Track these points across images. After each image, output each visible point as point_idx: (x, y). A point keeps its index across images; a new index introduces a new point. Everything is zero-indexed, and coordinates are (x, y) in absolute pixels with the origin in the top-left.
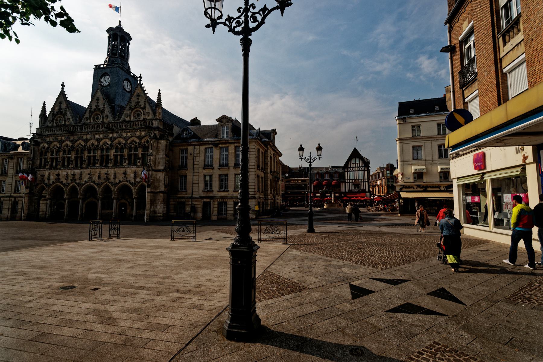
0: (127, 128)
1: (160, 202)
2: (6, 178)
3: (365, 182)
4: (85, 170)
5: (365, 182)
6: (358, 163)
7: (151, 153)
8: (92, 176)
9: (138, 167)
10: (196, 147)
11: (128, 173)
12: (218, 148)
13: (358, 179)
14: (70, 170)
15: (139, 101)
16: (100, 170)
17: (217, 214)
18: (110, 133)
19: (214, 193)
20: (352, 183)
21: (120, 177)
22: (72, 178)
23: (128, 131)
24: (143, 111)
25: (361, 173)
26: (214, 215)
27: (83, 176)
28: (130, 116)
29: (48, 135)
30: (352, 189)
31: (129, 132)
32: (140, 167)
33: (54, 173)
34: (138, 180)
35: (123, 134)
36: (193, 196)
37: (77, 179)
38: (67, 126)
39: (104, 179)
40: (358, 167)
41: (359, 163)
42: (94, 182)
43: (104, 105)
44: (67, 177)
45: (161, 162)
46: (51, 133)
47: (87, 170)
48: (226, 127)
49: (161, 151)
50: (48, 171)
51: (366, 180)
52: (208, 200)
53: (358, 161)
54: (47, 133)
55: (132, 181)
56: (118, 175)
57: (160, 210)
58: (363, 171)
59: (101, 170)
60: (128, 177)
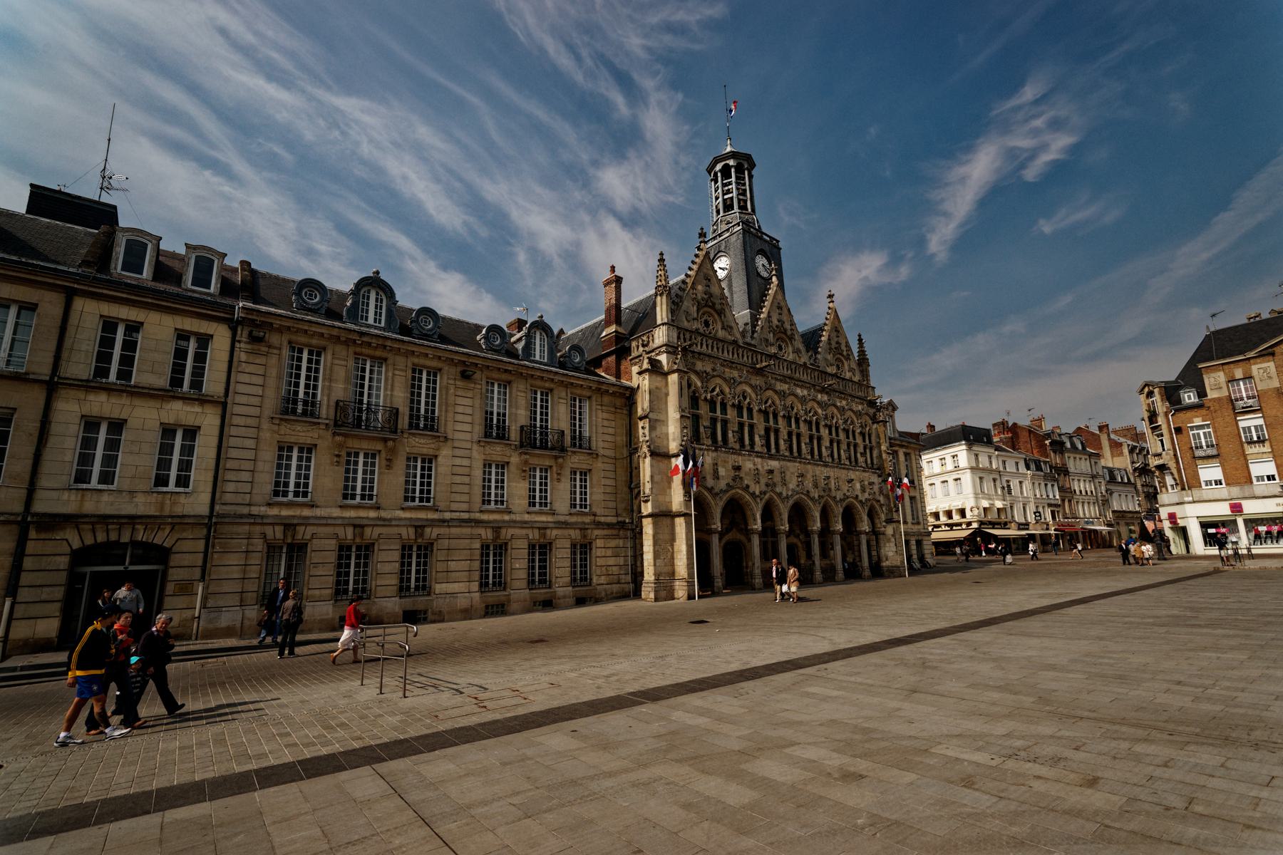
2: (438, 449)
29: (700, 354)
44: (757, 473)
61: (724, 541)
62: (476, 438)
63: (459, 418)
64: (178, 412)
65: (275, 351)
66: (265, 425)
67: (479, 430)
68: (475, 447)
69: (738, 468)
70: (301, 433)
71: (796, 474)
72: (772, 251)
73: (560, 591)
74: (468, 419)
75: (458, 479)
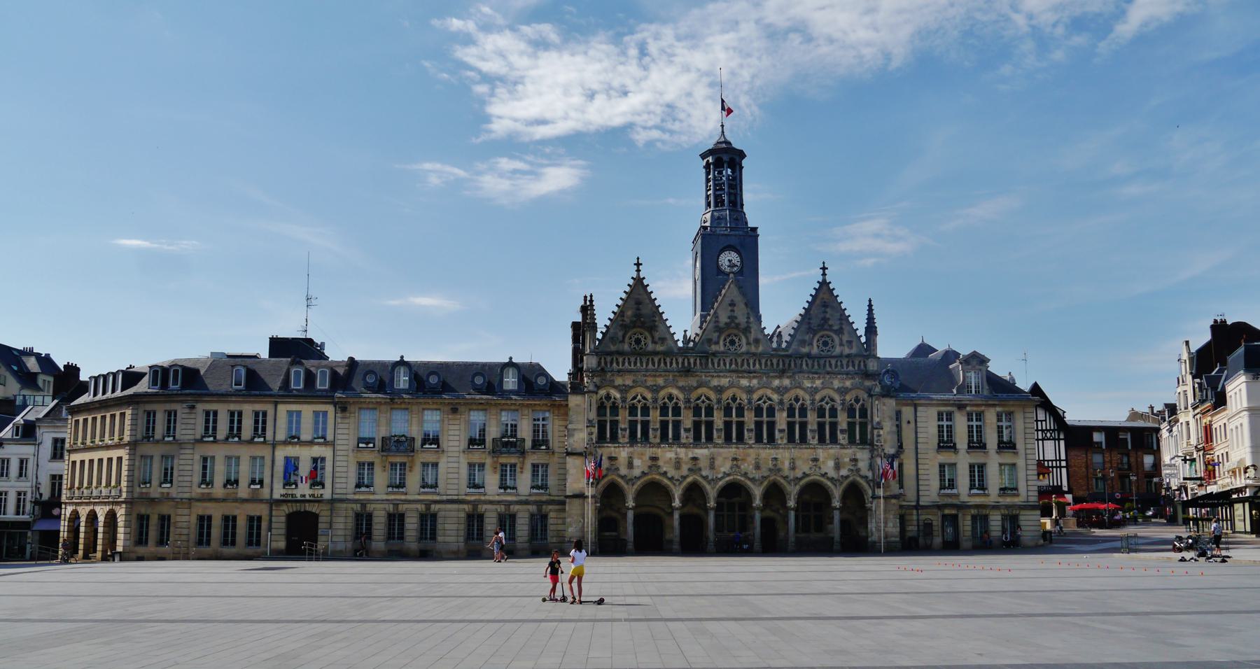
0: (813, 371)
1: (891, 517)
2: (439, 458)
3: (1061, 467)
4: (721, 450)
5: (1061, 467)
6: (1042, 421)
7: (878, 423)
8: (739, 462)
9: (844, 448)
11: (821, 460)
12: (964, 413)
15: (828, 316)
16: (757, 451)
17: (898, 539)
18: (776, 377)
21: (804, 467)
22: (689, 466)
23: (816, 376)
24: (841, 340)
25: (1049, 445)
27: (717, 463)
28: (811, 344)
29: (619, 371)
31: (819, 378)
32: (847, 448)
33: (642, 454)
34: (844, 472)
35: (805, 381)
36: (921, 503)
37: (703, 468)
39: (770, 470)
40: (1042, 431)
41: (1046, 421)
42: (745, 474)
43: (748, 318)
44: (678, 464)
47: (726, 450)
50: (626, 449)
51: (1064, 464)
52: (954, 512)
55: (832, 473)
56: (798, 463)
58: (1054, 439)
59: (761, 451)
60: (822, 467)
62: (462, 448)
63: (451, 438)
64: (317, 451)
65: (353, 415)
66: (351, 454)
67: (464, 444)
68: (462, 454)
69: (654, 459)
72: (746, 242)
73: (519, 546)
74: (457, 438)
75: (451, 476)
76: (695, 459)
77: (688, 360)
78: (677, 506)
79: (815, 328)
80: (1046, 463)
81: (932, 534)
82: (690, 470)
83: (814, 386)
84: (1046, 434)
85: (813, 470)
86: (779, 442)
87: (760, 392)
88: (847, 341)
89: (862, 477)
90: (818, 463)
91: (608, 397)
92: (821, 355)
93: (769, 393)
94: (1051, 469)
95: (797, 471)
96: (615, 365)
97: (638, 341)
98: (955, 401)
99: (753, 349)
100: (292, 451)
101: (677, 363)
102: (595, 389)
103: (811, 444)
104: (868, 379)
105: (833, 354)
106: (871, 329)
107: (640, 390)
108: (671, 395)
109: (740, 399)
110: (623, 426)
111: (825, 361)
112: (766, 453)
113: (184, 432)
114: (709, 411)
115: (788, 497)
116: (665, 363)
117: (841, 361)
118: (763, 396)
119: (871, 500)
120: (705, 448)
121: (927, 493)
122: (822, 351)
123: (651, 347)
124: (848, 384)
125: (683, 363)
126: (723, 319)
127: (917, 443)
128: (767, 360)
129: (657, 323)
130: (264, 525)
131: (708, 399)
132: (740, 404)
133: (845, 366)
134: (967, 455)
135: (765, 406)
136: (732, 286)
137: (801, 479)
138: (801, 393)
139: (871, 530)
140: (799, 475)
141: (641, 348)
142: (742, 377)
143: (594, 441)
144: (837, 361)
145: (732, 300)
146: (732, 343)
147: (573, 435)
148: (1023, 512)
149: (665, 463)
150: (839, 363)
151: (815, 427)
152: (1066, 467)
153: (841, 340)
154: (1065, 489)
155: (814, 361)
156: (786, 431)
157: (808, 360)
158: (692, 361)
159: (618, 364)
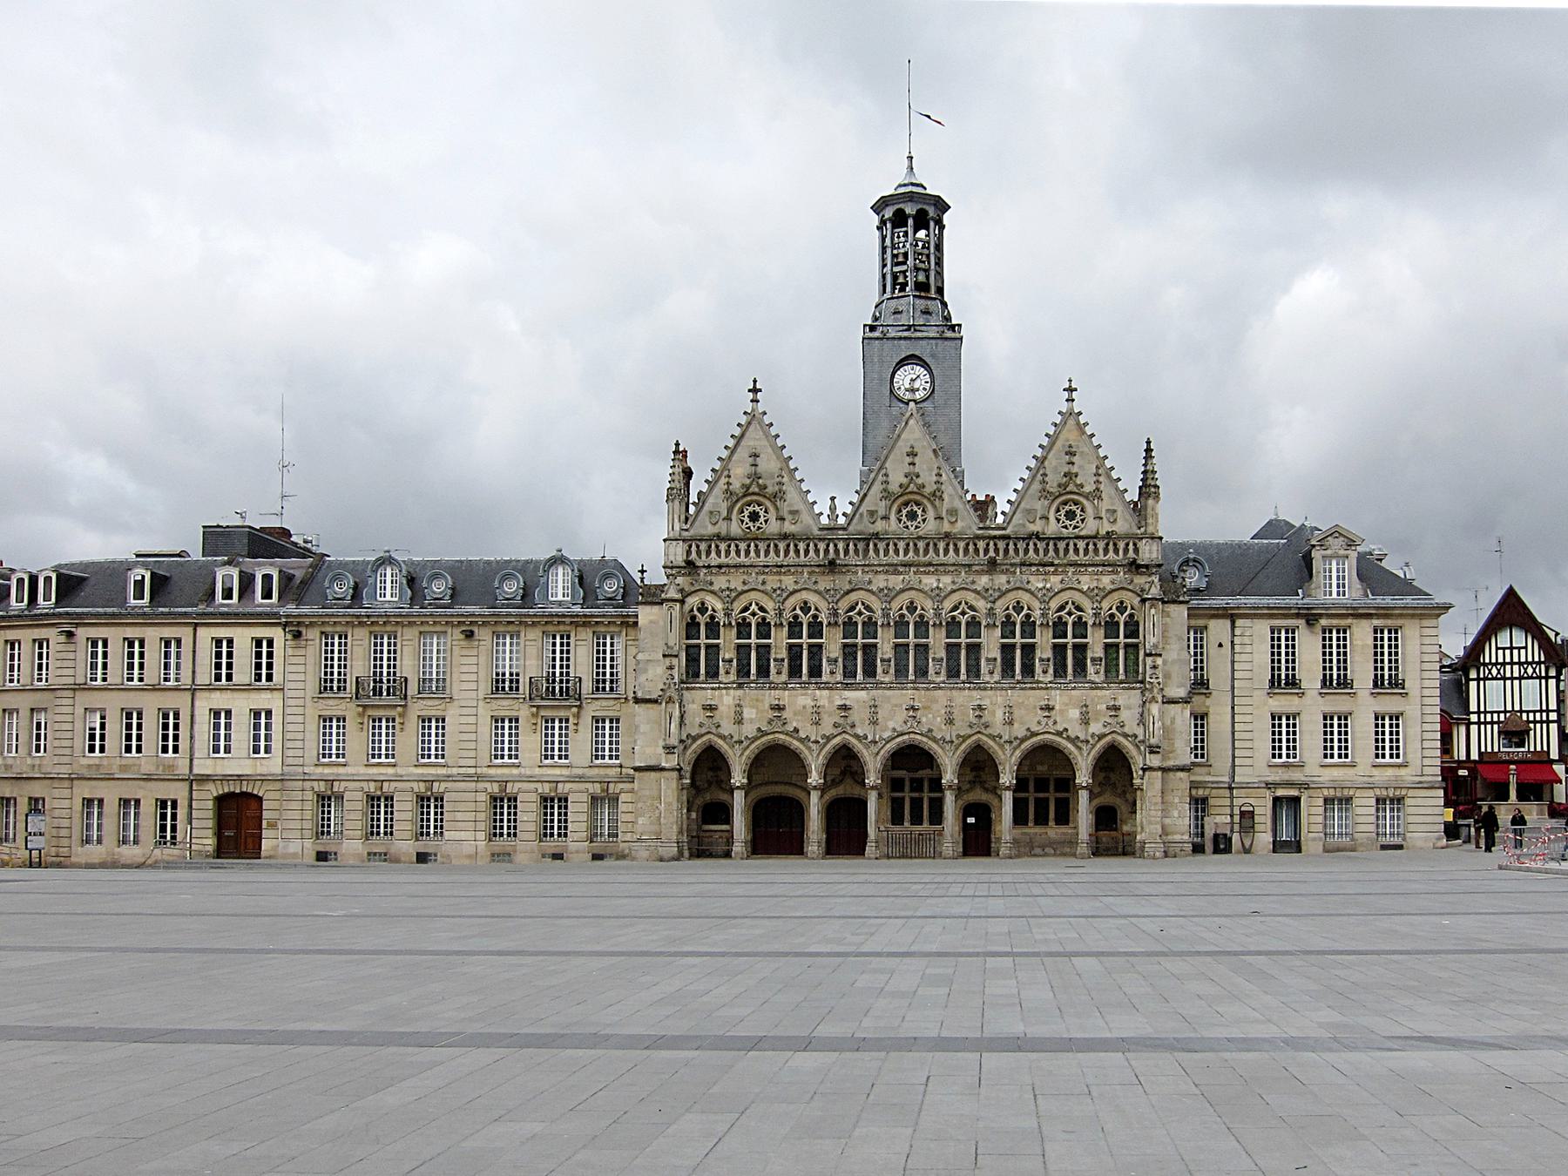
0: (1046, 559)
3: (1548, 722)
5: (1548, 722)
7: (1155, 646)
8: (919, 714)
9: (1097, 688)
10: (1239, 622)
11: (1057, 707)
12: (1318, 629)
13: (1521, 711)
14: (826, 692)
15: (1075, 469)
16: (949, 692)
19: (1307, 770)
20: (1496, 726)
23: (1052, 569)
24: (1096, 508)
25: (1531, 686)
26: (1314, 839)
27: (882, 714)
29: (720, 567)
30: (1496, 750)
31: (1055, 573)
32: (1103, 688)
34: (1096, 728)
35: (1032, 578)
38: (800, 540)
41: (1526, 648)
42: (929, 734)
45: (1174, 675)
46: (733, 559)
48: (1338, 564)
49: (1173, 640)
50: (732, 691)
51: (1553, 716)
52: (1294, 793)
53: (1519, 638)
54: (714, 559)
55: (1076, 730)
56: (1017, 713)
57: (1180, 822)
58: (1540, 678)
61: (827, 797)
66: (309, 703)
67: (485, 687)
68: (481, 703)
70: (334, 707)
71: (904, 707)
74: (474, 677)
76: (844, 708)
77: (836, 545)
78: (814, 784)
79: (1051, 490)
80: (1524, 715)
81: (1253, 827)
82: (836, 725)
83: (1048, 586)
84: (1525, 669)
85: (1044, 723)
86: (987, 678)
87: (955, 597)
88: (1108, 510)
89: (1126, 736)
90: (1053, 713)
91: (703, 609)
92: (1061, 533)
93: (971, 597)
94: (1532, 725)
95: (1016, 725)
96: (713, 554)
97: (754, 517)
98: (1299, 608)
99: (946, 527)
100: (220, 700)
101: (817, 551)
102: (679, 596)
103: (1041, 682)
104: (1142, 574)
105: (1082, 533)
106: (1148, 488)
107: (753, 595)
108: (806, 603)
109: (923, 609)
110: (727, 656)
111: (1068, 545)
112: (965, 699)
113: (59, 672)
114: (870, 627)
115: (1000, 768)
116: (797, 552)
117: (1095, 545)
118: (960, 603)
119: (1141, 772)
120: (862, 689)
121: (1248, 762)
122: (1066, 527)
123: (773, 527)
124: (1106, 581)
125: (827, 551)
126: (897, 478)
127: (1233, 679)
128: (968, 544)
129: (784, 488)
130: (182, 813)
131: (868, 608)
132: (921, 616)
133: (1101, 551)
134: (1319, 698)
135: (963, 620)
136: (912, 422)
137: (1023, 740)
138: (1025, 598)
139: (1142, 823)
140: (1021, 733)
141: (759, 528)
142: (928, 573)
143: (676, 680)
144: (1087, 545)
145: (912, 447)
146: (912, 516)
147: (646, 671)
148: (1411, 793)
149: (795, 714)
150: (1091, 547)
151: (1049, 654)
152: (1558, 721)
153: (1096, 508)
154: (1554, 755)
155: (1048, 545)
156: (999, 660)
157: (1038, 543)
158: (841, 546)
159: (718, 553)
